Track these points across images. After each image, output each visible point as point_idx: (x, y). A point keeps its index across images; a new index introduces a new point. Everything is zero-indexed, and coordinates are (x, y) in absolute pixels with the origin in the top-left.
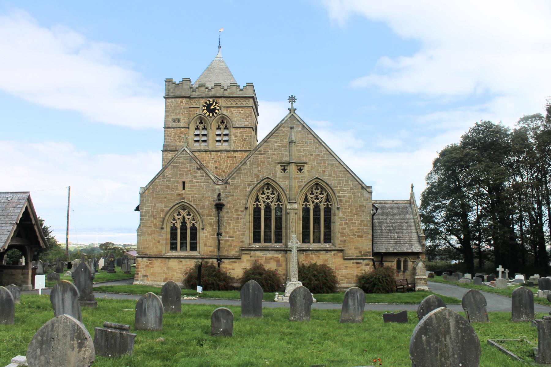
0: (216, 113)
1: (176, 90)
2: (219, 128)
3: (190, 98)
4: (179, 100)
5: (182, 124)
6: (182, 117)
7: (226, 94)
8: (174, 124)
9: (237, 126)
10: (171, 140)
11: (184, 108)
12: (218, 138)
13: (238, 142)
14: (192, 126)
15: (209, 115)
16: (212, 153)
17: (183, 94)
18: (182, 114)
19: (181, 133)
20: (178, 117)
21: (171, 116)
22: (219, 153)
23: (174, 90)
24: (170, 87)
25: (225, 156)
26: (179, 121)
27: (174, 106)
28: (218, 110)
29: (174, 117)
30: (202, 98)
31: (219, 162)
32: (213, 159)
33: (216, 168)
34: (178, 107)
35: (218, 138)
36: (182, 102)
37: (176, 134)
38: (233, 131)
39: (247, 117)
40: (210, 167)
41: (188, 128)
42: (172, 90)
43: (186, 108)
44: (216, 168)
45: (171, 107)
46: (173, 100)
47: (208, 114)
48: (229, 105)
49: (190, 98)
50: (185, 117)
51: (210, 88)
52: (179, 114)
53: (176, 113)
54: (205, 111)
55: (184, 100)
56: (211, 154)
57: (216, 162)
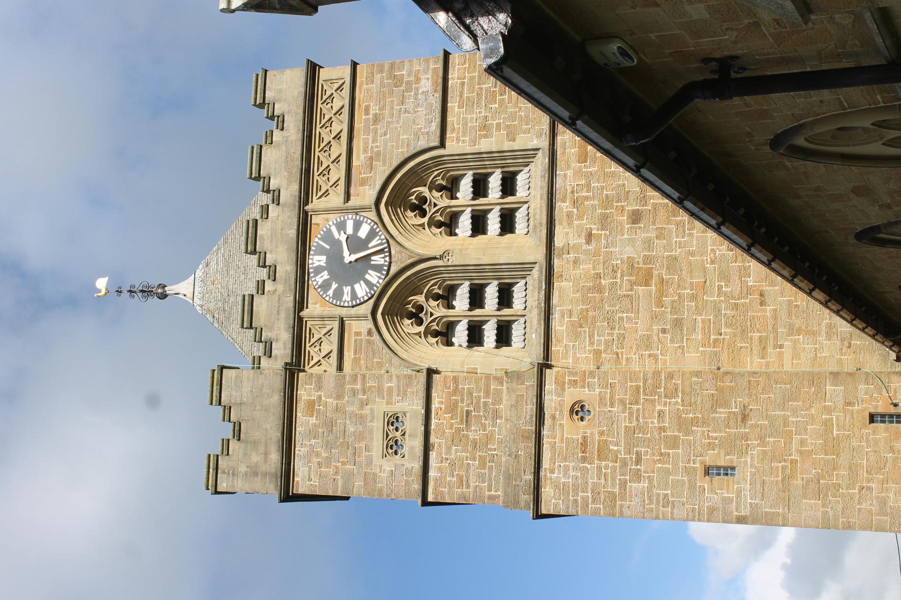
0: (372, 234)
1: (257, 435)
2: (449, 224)
3: (293, 369)
4: (303, 422)
5: (413, 406)
6: (381, 407)
7: (290, 191)
8: (413, 444)
9: (435, 126)
10: (482, 465)
11: (339, 397)
12: (493, 222)
13: (512, 117)
14: (430, 353)
15: (377, 268)
16: (558, 242)
17: (276, 399)
18: (363, 404)
19: (452, 408)
20: (377, 426)
21: (370, 462)
22: (562, 207)
23: (255, 444)
24: (243, 469)
25: (578, 173)
26: (394, 420)
27: (328, 446)
28: (357, 226)
29: (378, 443)
30: (301, 303)
31: (607, 202)
32: (589, 237)
33: (636, 217)
34: (330, 424)
35: (493, 222)
36: (311, 405)
37: (458, 438)
38: (453, 147)
39: (398, 81)
40: (629, 252)
41: (431, 372)
42: (255, 458)
43: (340, 385)
44: (636, 217)
45: (328, 460)
46: (300, 450)
47: (373, 277)
48: (338, 173)
49: (293, 369)
50: (380, 390)
51: (263, 273)
52: (361, 419)
53: (360, 437)
54: (361, 290)
55: (305, 392)
56: (567, 249)
57: (604, 222)
